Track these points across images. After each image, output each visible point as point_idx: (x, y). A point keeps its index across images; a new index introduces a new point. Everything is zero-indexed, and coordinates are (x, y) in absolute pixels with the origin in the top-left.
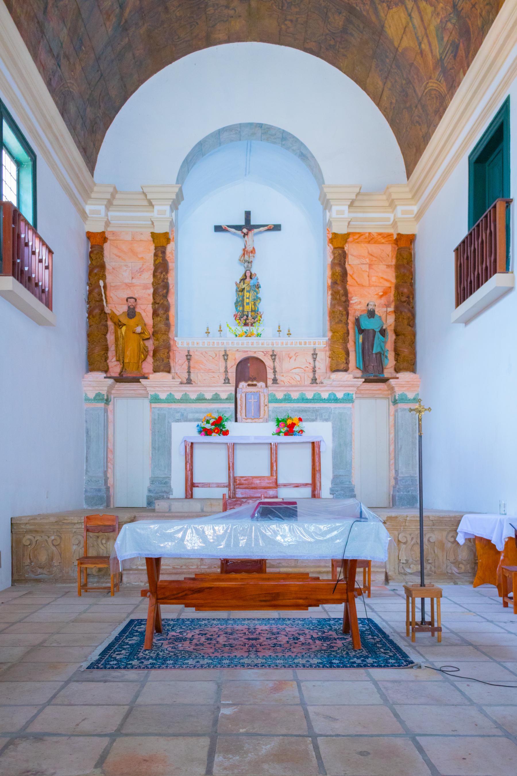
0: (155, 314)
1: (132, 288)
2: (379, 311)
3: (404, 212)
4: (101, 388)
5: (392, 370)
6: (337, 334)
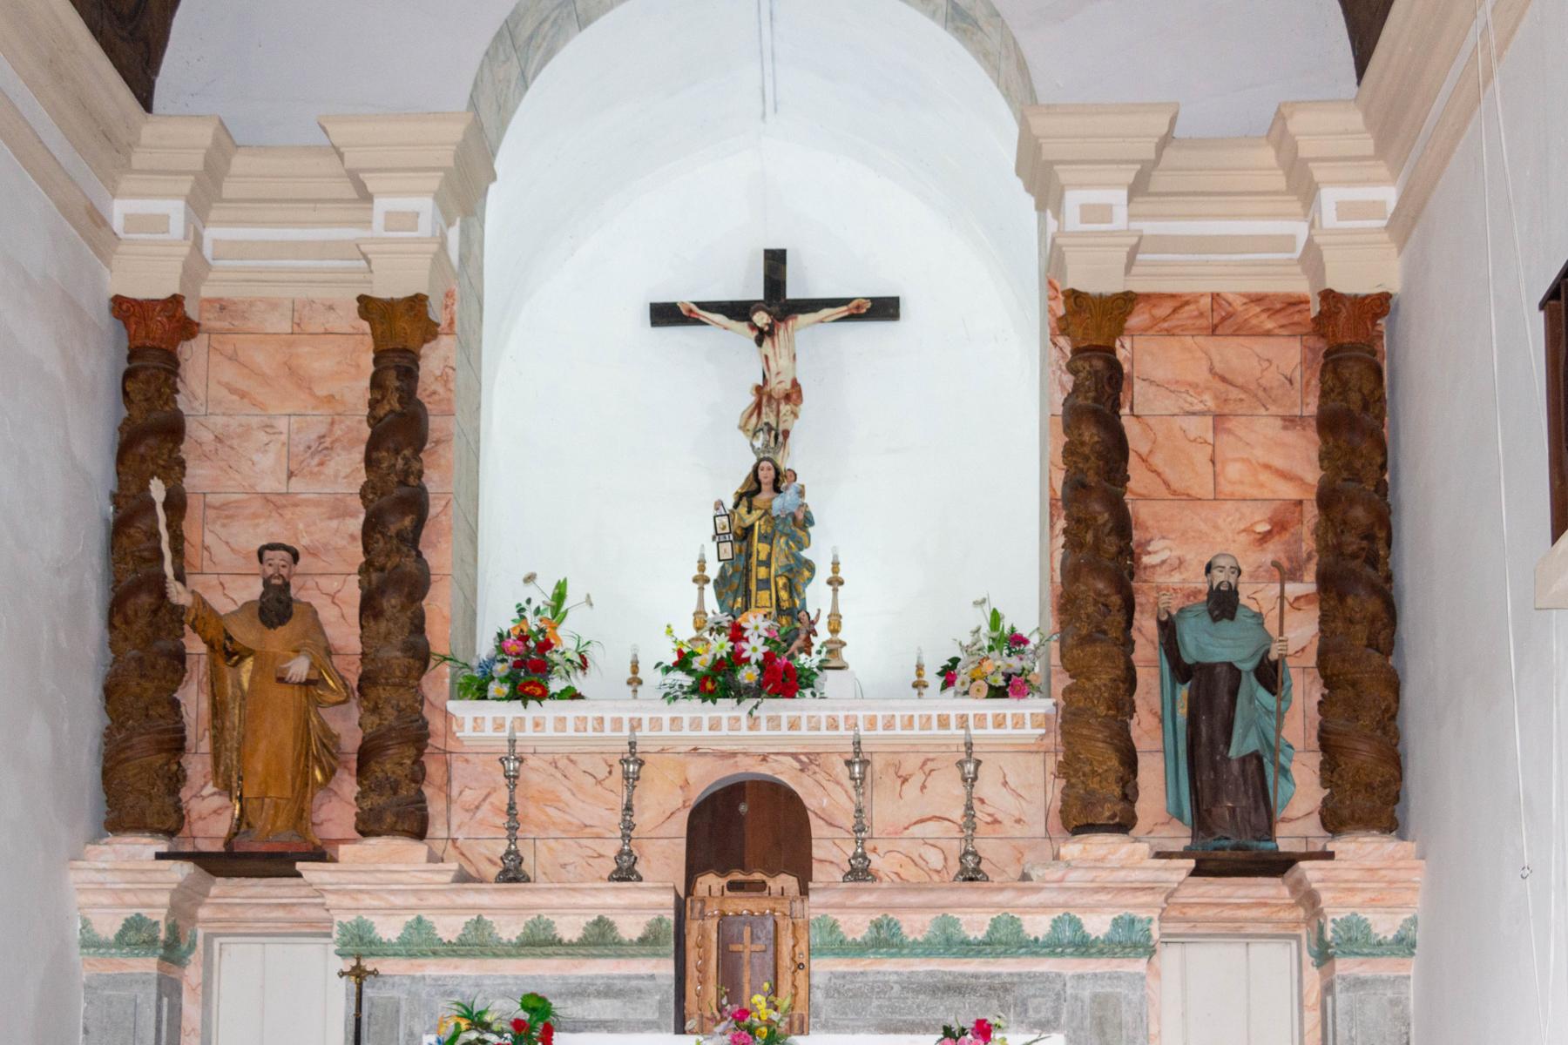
0: (370, 607)
1: (288, 514)
3: (1345, 210)
4: (145, 898)
5: (1313, 826)
6: (1088, 685)
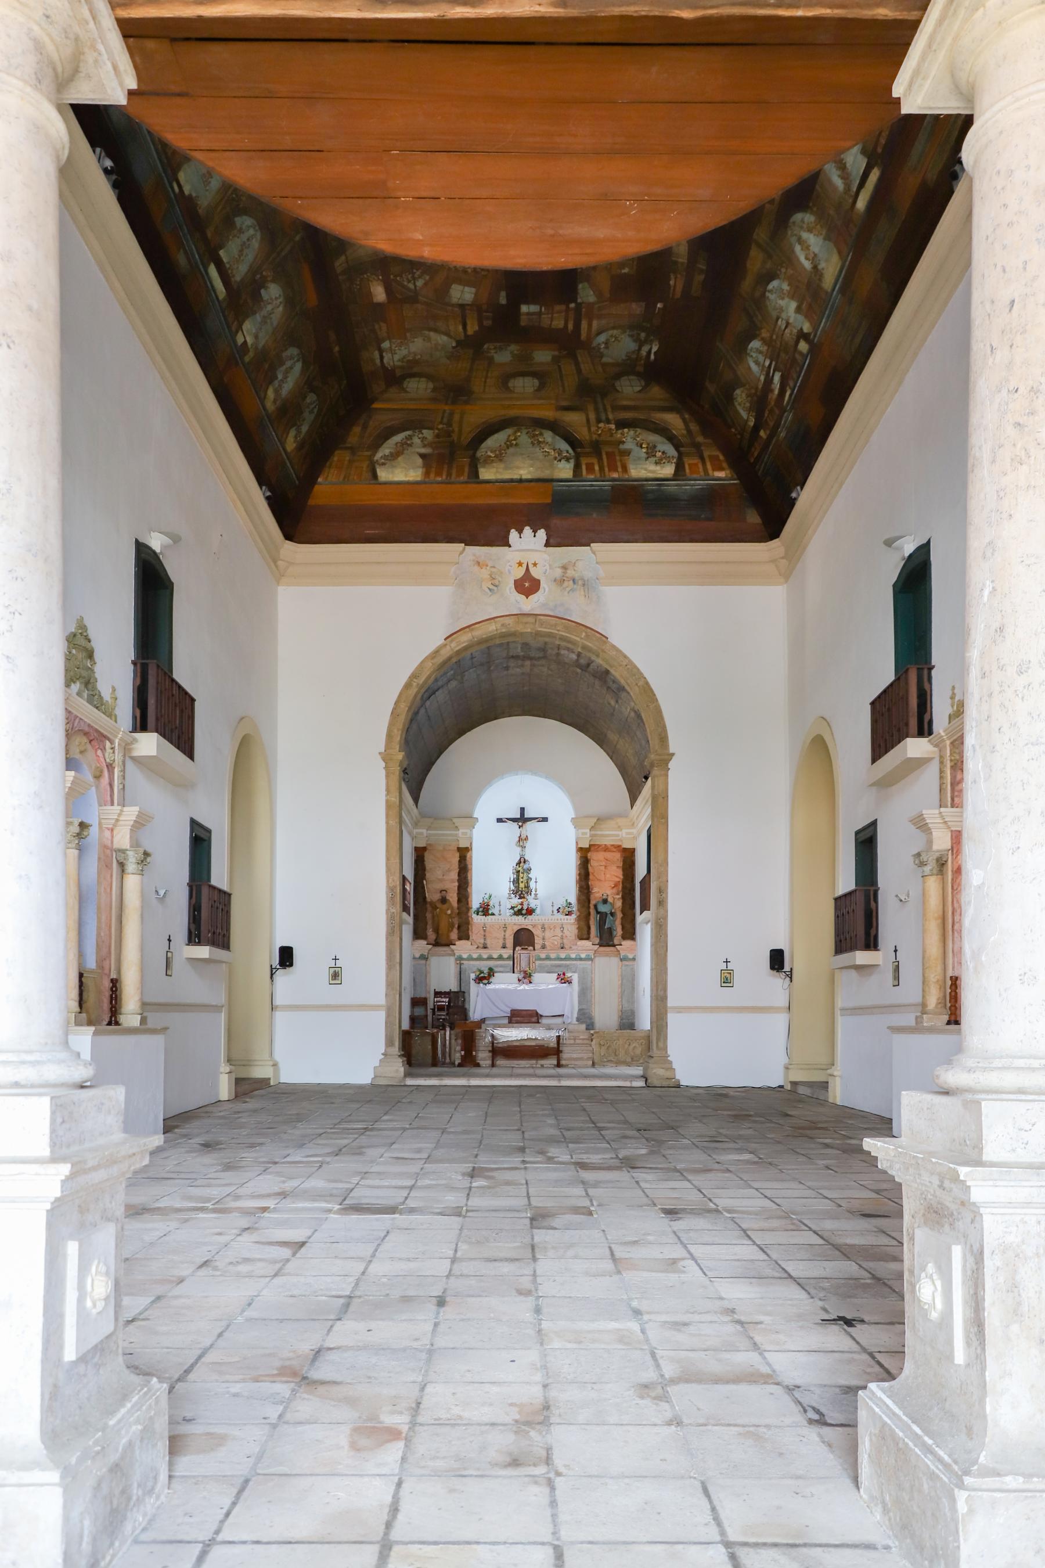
2: (610, 900)
